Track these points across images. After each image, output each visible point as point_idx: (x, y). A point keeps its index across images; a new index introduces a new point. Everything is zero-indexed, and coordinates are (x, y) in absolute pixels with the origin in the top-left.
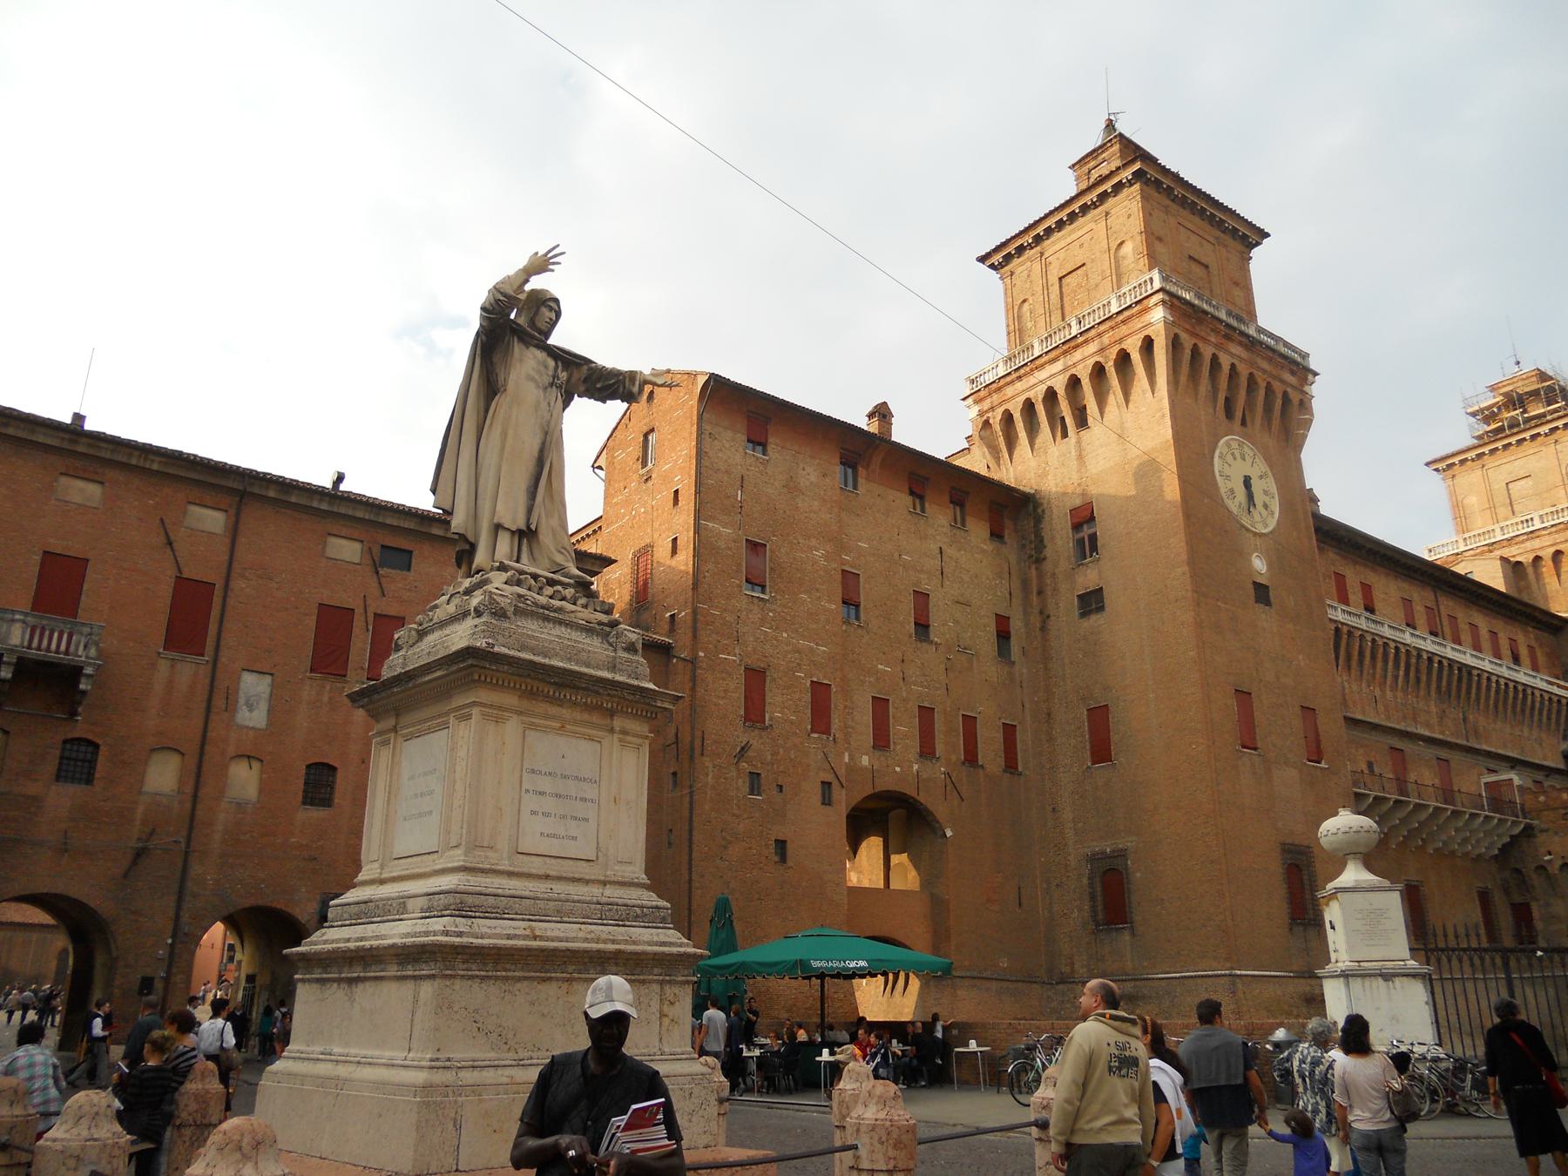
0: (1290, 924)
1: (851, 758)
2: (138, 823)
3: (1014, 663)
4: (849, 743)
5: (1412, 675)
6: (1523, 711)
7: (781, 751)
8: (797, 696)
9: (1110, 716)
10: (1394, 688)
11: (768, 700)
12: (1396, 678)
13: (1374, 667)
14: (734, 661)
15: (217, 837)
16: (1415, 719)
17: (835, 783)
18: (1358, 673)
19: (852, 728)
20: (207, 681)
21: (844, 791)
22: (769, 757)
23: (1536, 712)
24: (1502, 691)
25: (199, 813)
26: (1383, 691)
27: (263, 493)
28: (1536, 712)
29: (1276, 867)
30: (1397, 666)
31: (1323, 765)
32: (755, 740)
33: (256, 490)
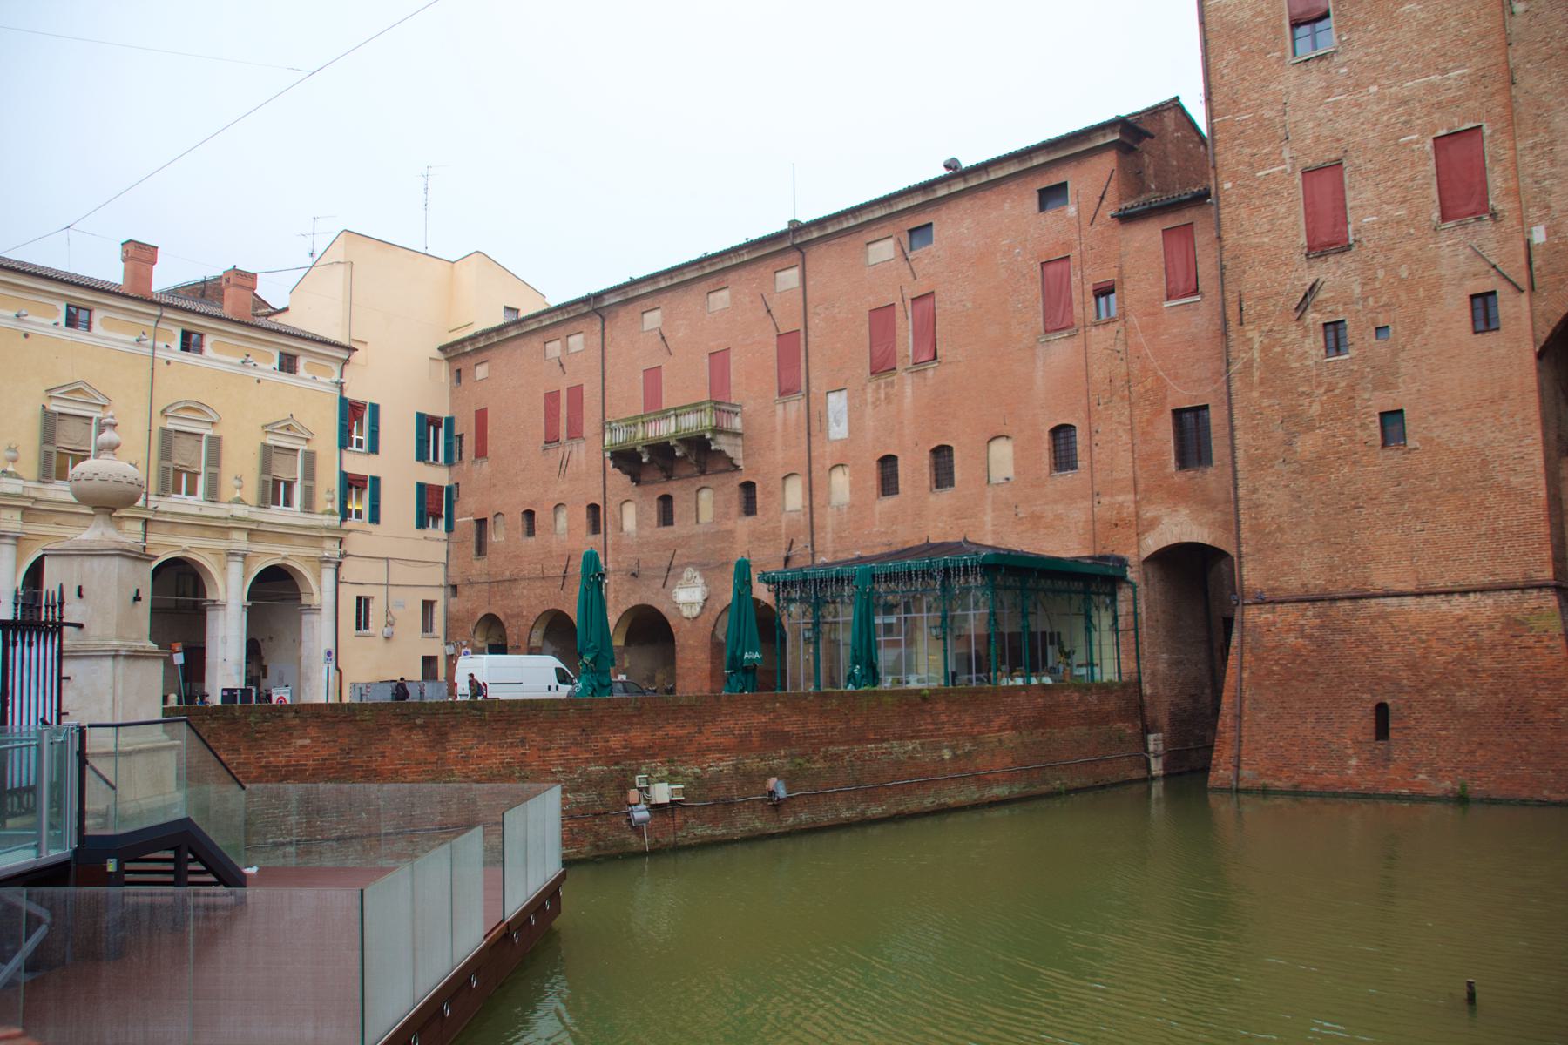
1: (1550, 232)
2: (784, 537)
4: (1548, 207)
7: (1381, 274)
8: (1401, 177)
11: (1349, 204)
14: (1283, 171)
15: (829, 536)
17: (1503, 291)
19: (1553, 176)
20: (805, 412)
21: (1524, 298)
22: (1357, 290)
25: (815, 520)
27: (810, 237)
32: (1330, 272)
33: (806, 238)
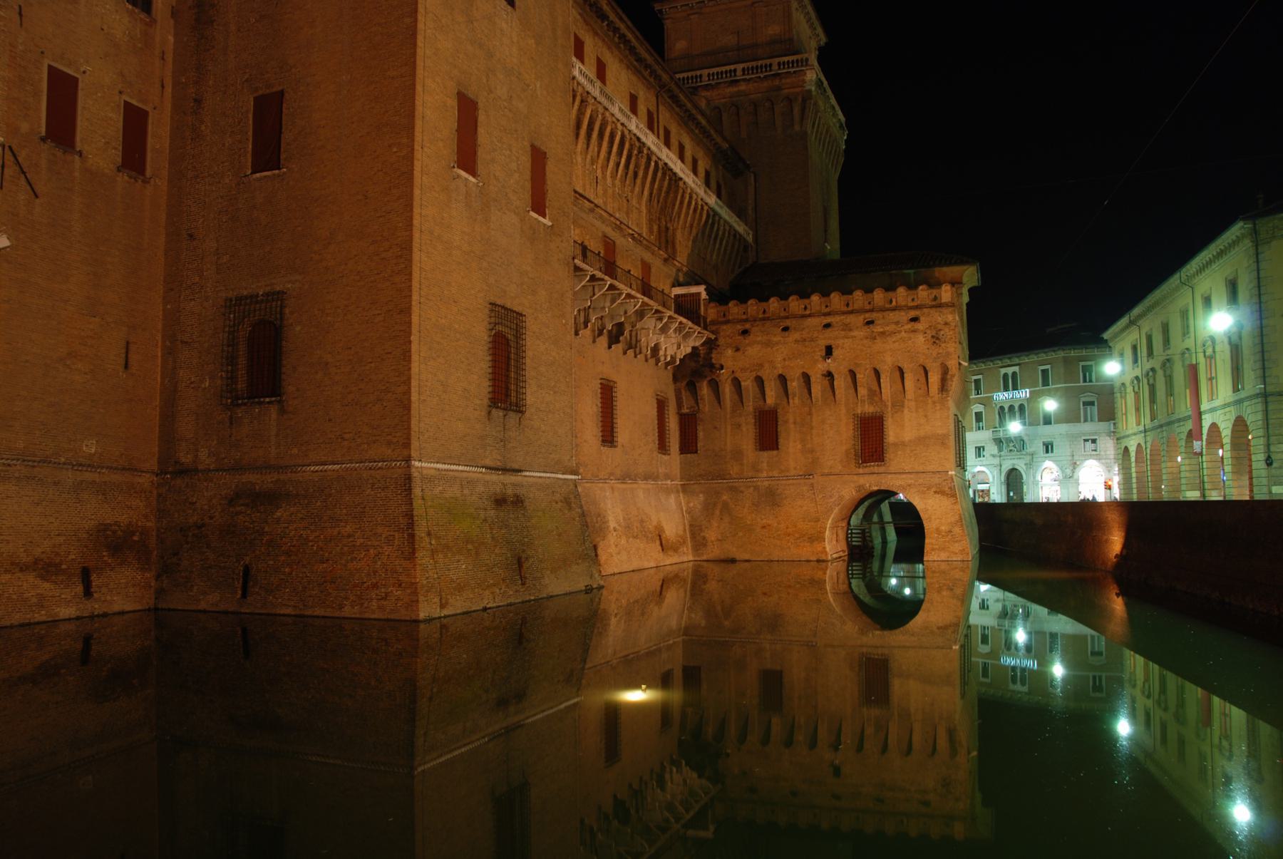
0: (490, 406)
3: (155, 21)
5: (632, 167)
6: (710, 236)
9: (284, 105)
10: (614, 176)
12: (618, 165)
13: (600, 146)
16: (627, 214)
18: (585, 146)
23: (718, 241)
24: (698, 211)
26: (604, 177)
28: (718, 241)
29: (481, 333)
30: (620, 154)
31: (547, 222)
